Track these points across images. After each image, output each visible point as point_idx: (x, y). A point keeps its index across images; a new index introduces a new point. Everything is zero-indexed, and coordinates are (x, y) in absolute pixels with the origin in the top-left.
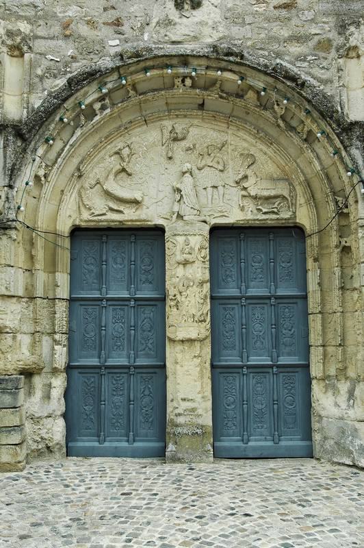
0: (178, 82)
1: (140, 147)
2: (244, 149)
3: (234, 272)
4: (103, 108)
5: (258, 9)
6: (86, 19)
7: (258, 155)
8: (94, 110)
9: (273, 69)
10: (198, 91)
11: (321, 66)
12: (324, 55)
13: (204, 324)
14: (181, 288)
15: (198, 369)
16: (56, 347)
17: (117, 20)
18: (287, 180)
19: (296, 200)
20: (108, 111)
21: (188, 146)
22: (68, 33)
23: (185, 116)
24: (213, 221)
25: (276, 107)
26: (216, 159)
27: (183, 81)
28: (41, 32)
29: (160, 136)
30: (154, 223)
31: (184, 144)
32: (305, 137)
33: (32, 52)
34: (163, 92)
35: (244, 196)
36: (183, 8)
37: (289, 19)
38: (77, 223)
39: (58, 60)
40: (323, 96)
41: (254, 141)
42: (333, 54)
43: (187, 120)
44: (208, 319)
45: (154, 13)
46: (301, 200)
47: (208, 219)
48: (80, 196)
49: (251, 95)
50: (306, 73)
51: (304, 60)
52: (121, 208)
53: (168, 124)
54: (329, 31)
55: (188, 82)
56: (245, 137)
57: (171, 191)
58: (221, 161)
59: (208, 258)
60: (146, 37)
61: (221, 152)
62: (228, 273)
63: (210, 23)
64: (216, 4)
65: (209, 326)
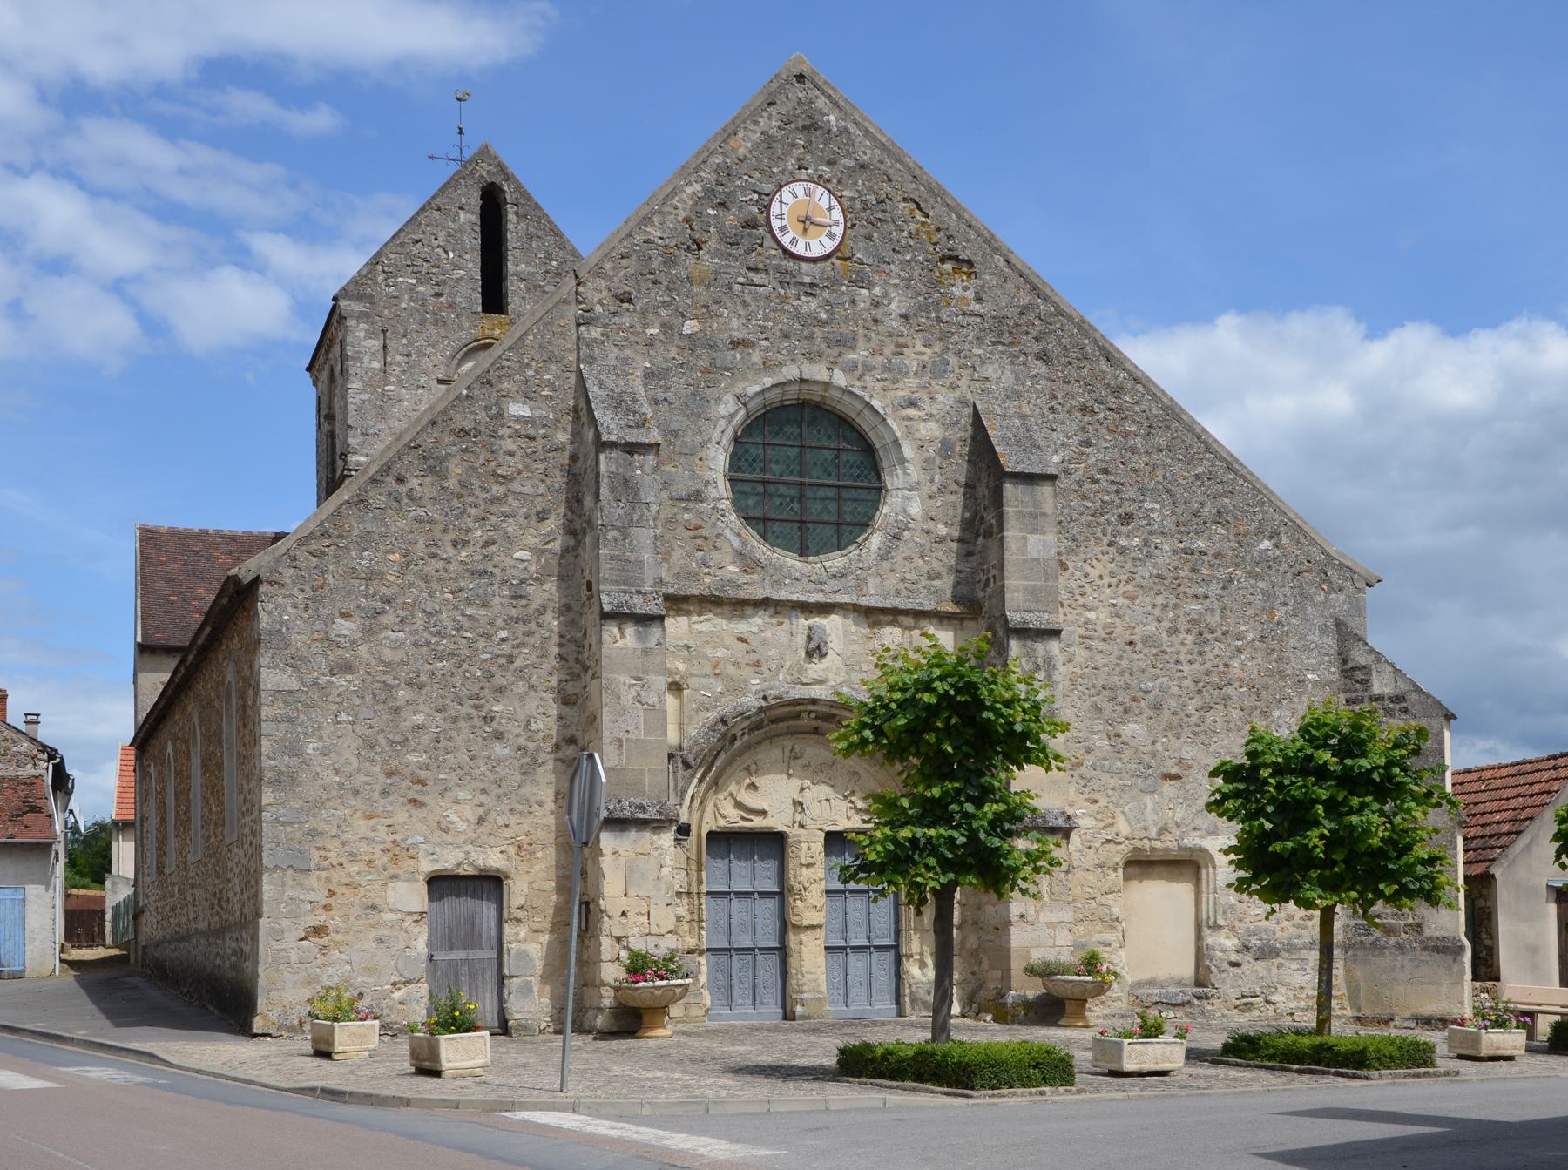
22: (717, 671)
24: (827, 829)
28: (695, 669)
38: (714, 829)
48: (716, 806)
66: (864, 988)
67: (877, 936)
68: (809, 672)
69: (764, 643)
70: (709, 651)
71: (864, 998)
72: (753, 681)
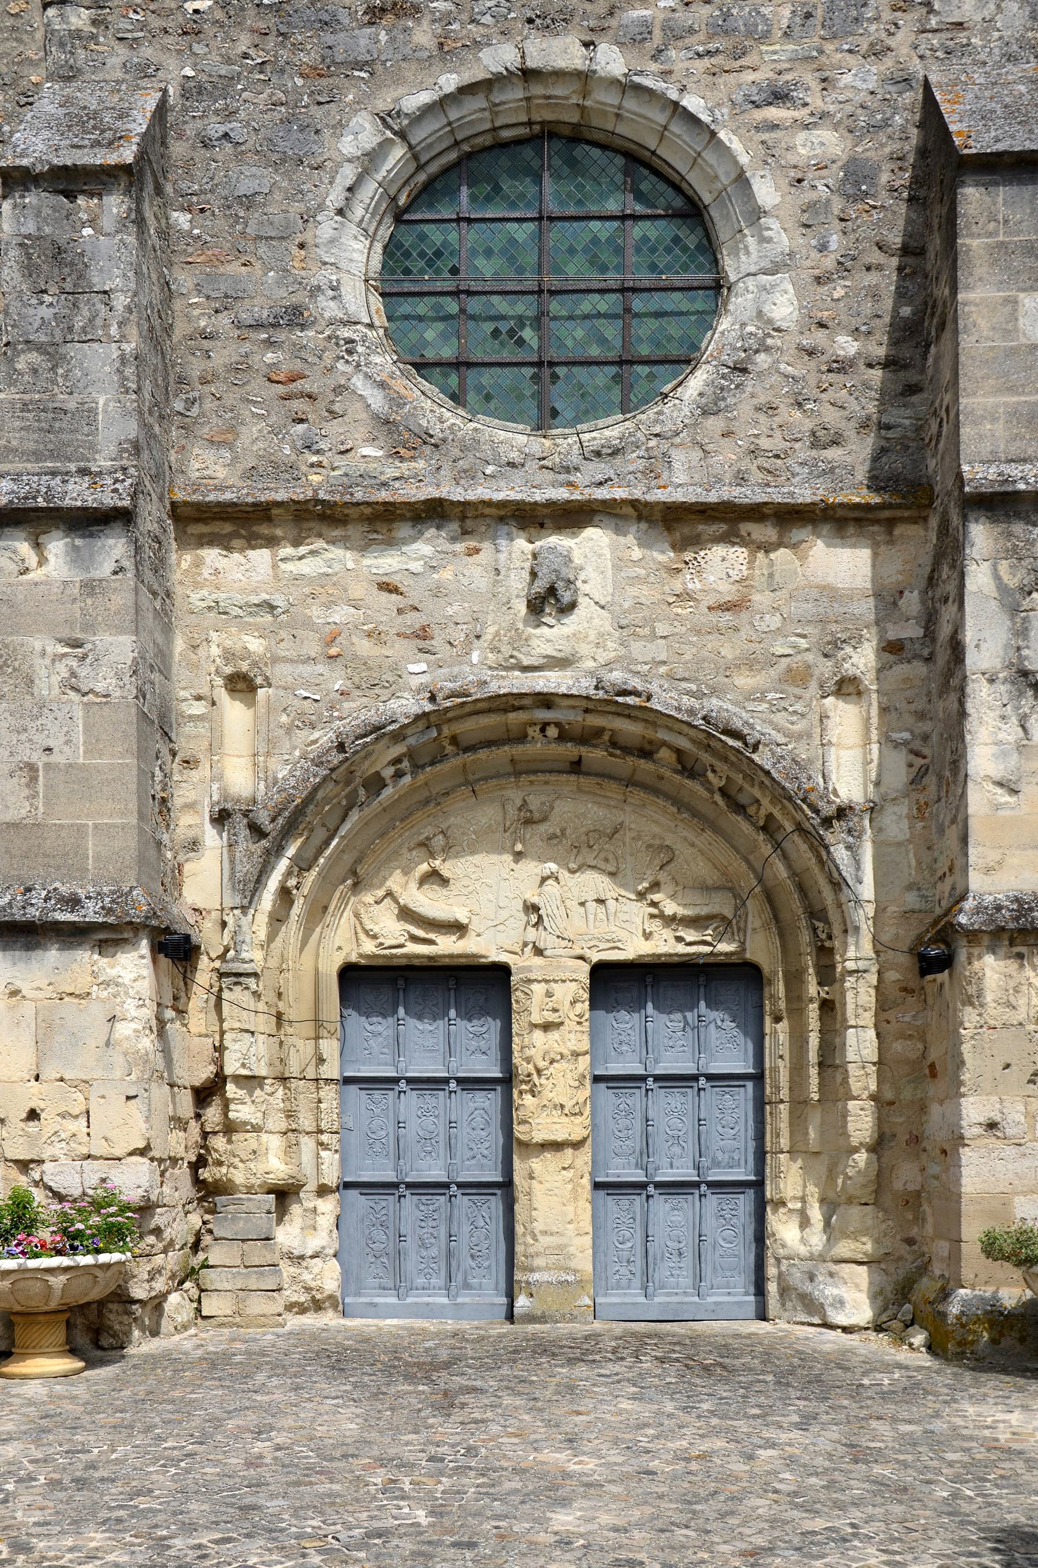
0: (533, 732)
1: (463, 834)
2: (654, 837)
3: (636, 1037)
4: (399, 775)
5: (679, 611)
6: (365, 628)
7: (680, 847)
8: (383, 779)
9: (704, 718)
10: (569, 745)
11: (791, 709)
12: (797, 691)
13: (578, 1120)
17: (423, 629)
18: (731, 889)
19: (746, 922)
21: (551, 831)
22: (333, 651)
23: (546, 783)
24: (596, 957)
25: (710, 774)
26: (602, 855)
27: (543, 730)
29: (501, 815)
30: (490, 960)
31: (542, 828)
32: (761, 823)
33: (270, 685)
34: (506, 748)
35: (652, 916)
36: (542, 611)
37: (737, 630)
38: (354, 958)
39: (317, 697)
40: (793, 760)
41: (673, 825)
42: (813, 687)
43: (550, 788)
44: (587, 1111)
45: (490, 617)
46: (754, 921)
47: (588, 953)
48: (357, 916)
49: (664, 754)
50: (764, 721)
51: (762, 700)
52: (432, 936)
53: (516, 796)
54: (807, 650)
55: (552, 732)
56: (656, 816)
57: (520, 907)
58: (611, 857)
59: (587, 1016)
60: (475, 657)
61: (613, 841)
62: (622, 1038)
63: (592, 637)
64: (602, 603)
67: (716, 1164)
68: (534, 642)
69: (437, 592)
70: (316, 613)
72: (413, 668)
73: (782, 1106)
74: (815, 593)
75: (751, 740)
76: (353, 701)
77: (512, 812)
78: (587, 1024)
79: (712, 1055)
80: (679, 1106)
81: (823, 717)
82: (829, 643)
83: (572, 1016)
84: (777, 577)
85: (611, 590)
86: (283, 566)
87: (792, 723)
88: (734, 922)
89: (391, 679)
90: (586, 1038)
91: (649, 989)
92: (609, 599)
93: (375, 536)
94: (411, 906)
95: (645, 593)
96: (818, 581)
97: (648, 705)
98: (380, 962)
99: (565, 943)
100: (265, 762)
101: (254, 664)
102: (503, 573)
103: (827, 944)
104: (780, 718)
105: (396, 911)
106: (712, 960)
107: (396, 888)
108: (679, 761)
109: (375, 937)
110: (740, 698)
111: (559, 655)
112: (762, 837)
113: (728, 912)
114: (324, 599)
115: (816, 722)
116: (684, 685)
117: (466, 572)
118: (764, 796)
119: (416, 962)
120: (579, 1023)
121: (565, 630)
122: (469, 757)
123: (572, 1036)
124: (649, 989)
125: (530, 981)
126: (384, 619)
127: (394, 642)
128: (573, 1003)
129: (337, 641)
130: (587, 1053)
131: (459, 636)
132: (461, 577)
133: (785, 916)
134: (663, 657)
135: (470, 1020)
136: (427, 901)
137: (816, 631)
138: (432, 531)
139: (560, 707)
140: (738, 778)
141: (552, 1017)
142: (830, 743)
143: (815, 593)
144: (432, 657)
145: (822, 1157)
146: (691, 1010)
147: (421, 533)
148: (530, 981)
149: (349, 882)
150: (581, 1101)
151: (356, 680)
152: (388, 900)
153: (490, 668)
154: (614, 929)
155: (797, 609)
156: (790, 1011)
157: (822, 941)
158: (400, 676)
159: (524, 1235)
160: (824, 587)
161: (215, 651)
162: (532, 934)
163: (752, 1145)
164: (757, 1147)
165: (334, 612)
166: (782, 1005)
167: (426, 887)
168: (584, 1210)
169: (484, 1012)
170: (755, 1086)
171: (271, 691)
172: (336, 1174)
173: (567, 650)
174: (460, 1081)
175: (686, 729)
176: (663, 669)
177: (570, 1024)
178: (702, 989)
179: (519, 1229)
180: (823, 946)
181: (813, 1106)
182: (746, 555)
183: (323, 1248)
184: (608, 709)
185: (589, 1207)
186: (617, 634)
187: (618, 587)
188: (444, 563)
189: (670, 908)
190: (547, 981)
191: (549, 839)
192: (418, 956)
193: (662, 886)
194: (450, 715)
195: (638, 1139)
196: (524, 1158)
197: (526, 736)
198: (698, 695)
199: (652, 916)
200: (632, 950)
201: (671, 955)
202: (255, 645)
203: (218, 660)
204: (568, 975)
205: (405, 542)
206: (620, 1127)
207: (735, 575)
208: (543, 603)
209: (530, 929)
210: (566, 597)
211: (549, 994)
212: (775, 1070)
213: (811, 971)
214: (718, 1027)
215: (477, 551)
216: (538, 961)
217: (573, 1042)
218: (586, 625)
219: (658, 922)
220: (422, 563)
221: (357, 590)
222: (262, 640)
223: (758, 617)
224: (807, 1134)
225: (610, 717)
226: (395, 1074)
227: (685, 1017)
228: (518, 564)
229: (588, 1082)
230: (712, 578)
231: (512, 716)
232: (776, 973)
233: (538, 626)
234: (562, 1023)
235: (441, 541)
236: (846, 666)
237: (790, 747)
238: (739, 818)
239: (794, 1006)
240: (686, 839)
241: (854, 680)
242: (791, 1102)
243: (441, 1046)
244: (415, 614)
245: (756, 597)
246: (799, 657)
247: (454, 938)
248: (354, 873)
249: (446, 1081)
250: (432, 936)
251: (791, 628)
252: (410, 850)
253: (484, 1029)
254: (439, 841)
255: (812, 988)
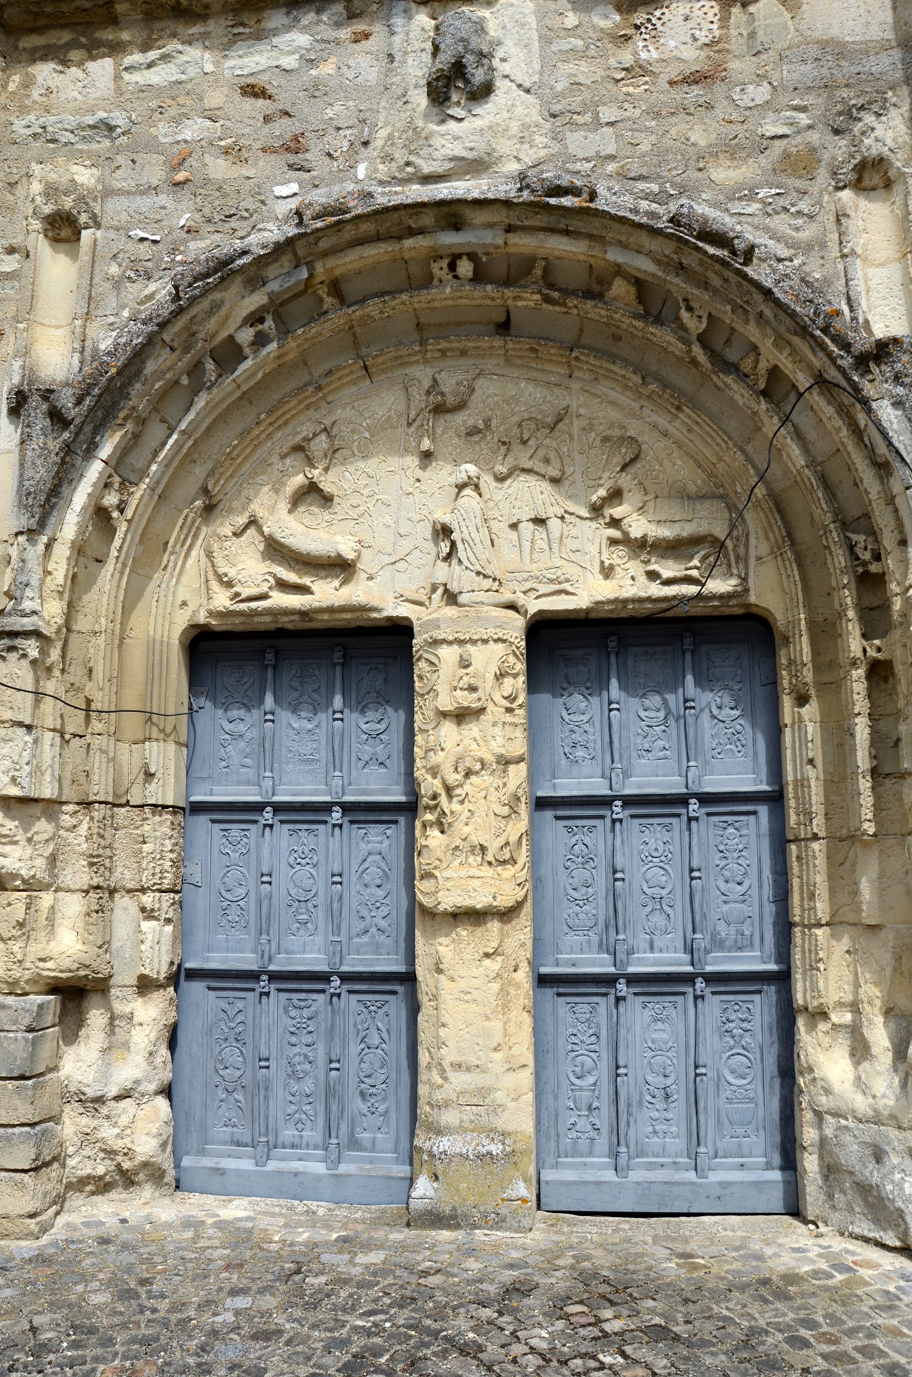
0: (440, 269)
1: (353, 431)
2: (612, 425)
3: (595, 735)
4: (260, 340)
5: (631, 89)
6: (223, 143)
7: (648, 439)
8: (239, 348)
9: (671, 220)
10: (489, 287)
11: (793, 210)
12: (800, 183)
13: (509, 871)
14: (453, 778)
15: (495, 986)
16: (146, 926)
17: (296, 139)
18: (722, 497)
19: (747, 546)
20: (273, 346)
21: (471, 422)
22: (180, 176)
23: (463, 353)
24: (534, 606)
25: (684, 314)
26: (541, 453)
27: (452, 267)
28: (122, 179)
29: (403, 401)
30: (385, 614)
31: (460, 419)
32: (762, 385)
33: (98, 226)
34: (404, 297)
35: (613, 542)
36: (448, 99)
37: (709, 107)
38: (202, 618)
39: (157, 238)
40: (803, 280)
41: (636, 405)
42: (823, 176)
43: (467, 362)
44: (523, 857)
45: (381, 118)
46: (758, 546)
47: (521, 600)
48: (209, 555)
49: (620, 289)
50: (757, 228)
51: (751, 197)
52: (306, 581)
53: (422, 374)
54: (810, 127)
55: (465, 268)
56: (614, 395)
57: (428, 533)
58: (552, 455)
59: (521, 699)
60: (361, 171)
61: (556, 433)
62: (576, 737)
63: (515, 127)
64: (527, 84)
65: (523, 875)
66: (679, 1108)
67: (718, 943)
68: (437, 141)
69: (315, 91)
70: (163, 131)
71: (676, 1143)
72: (280, 190)
73: (816, 846)
74: (814, 51)
75: (739, 245)
76: (202, 239)
77: (417, 395)
78: (522, 712)
79: (706, 762)
80: (661, 847)
81: (840, 217)
82: (840, 113)
83: (497, 697)
84: (761, 36)
85: (537, 67)
86: (126, 76)
87: (797, 229)
88: (729, 544)
89: (251, 207)
90: (520, 734)
91: (613, 660)
92: (536, 78)
93: (241, 30)
94: (278, 536)
95: (584, 71)
96: (817, 34)
97: (592, 205)
98: (235, 624)
99: (487, 583)
100: (84, 327)
101: (81, 199)
102: (398, 58)
103: (874, 568)
104: (780, 223)
105: (261, 547)
106: (698, 609)
107: (261, 513)
108: (641, 297)
109: (229, 585)
110: (721, 198)
111: (470, 155)
112: (764, 406)
113: (720, 531)
114: (172, 112)
115: (831, 225)
116: (641, 185)
117: (351, 62)
118: (764, 336)
119: (285, 622)
120: (509, 710)
121: (478, 123)
122: (357, 313)
123: (498, 730)
124: (613, 660)
125: (436, 643)
126: (247, 130)
127: (257, 159)
128: (500, 676)
129: (186, 164)
130: (521, 759)
131: (341, 143)
132: (344, 70)
133: (804, 534)
134: (611, 149)
135: (362, 712)
136: (301, 528)
137: (820, 101)
138: (311, 16)
139: (472, 226)
140: (725, 312)
141: (467, 700)
142: (853, 252)
143: (814, 51)
144: (306, 176)
145: (883, 933)
146: (674, 690)
147: (297, 20)
148: (436, 643)
149: (198, 503)
150: (513, 839)
151: (207, 211)
152: (251, 531)
153: (381, 183)
154: (559, 562)
155: (789, 73)
156: (821, 686)
157: (864, 564)
158: (263, 202)
159: (429, 1067)
160: (827, 42)
161: (36, 187)
162: (442, 573)
163: (770, 910)
164: (777, 914)
165: (186, 127)
166: (808, 675)
167: (302, 509)
168: (520, 1025)
169: (382, 699)
170: (771, 812)
171: (99, 234)
172: (166, 959)
173: (481, 146)
174: (347, 808)
175: (645, 240)
176: (611, 167)
177: (495, 712)
178: (688, 656)
179: (423, 1058)
180: (866, 573)
181: (866, 844)
182: (716, 9)
183: (137, 1082)
184: (536, 222)
185: (527, 1020)
186: (548, 126)
187: (548, 64)
188: (325, 55)
189: (638, 527)
190: (461, 642)
191: (469, 434)
192: (286, 612)
193: (626, 495)
194: (324, 244)
195: (602, 902)
196: (432, 934)
197: (431, 277)
198: (660, 198)
199: (613, 542)
200: (585, 594)
201: (641, 600)
202: (85, 176)
203: (39, 199)
204: (491, 632)
205: (275, 32)
206: (576, 882)
207: (703, 37)
208: (447, 86)
209: (439, 562)
210: (478, 76)
211: (465, 664)
212: (802, 783)
213: (851, 614)
214: (714, 717)
215: (367, 36)
216: (451, 611)
217: (500, 740)
218: (505, 115)
219: (621, 551)
220: (297, 56)
221: (215, 98)
222: (94, 170)
223: (738, 89)
224: (856, 893)
225: (541, 235)
226: (258, 799)
227: (665, 702)
228: (417, 45)
229: (523, 809)
230: (672, 43)
231: (408, 243)
232: (795, 623)
233: (443, 121)
234: (482, 710)
235: (321, 27)
236: (867, 142)
237: (796, 262)
238: (729, 380)
239: (826, 678)
240: (655, 426)
241: (879, 163)
242: (832, 838)
243: (323, 755)
244: (286, 121)
245: (734, 65)
246: (799, 139)
247: (336, 583)
248: (205, 491)
249: (326, 808)
250: (306, 581)
251: (784, 99)
252: (283, 457)
253: (382, 727)
254: (321, 443)
255: (855, 644)
